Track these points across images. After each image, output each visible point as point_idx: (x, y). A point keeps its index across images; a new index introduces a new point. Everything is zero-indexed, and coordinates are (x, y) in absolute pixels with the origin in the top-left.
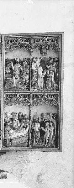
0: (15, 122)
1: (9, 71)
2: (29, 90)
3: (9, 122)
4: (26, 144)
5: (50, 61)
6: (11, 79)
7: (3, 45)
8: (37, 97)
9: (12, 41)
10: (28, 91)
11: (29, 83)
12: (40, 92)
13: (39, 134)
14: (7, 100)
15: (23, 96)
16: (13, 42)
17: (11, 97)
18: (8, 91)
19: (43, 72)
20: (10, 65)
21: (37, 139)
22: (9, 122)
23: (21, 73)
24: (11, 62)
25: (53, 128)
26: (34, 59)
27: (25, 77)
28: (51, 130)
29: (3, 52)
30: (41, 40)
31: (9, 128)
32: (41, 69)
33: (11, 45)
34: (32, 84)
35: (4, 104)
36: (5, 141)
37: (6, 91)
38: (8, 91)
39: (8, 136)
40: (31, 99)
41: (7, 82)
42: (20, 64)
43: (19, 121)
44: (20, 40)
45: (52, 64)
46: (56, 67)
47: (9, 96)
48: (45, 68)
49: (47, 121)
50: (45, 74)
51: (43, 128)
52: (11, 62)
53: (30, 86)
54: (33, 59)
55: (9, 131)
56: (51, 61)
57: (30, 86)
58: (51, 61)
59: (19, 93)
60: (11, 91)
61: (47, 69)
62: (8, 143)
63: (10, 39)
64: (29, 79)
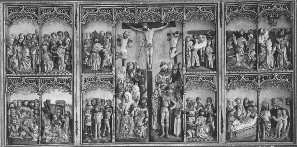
0: (239, 110)
1: (231, 47)
2: (256, 69)
3: (232, 110)
4: (254, 138)
5: (281, 33)
6: (234, 57)
7: (223, 14)
8: (266, 78)
9: (234, 8)
10: (255, 72)
11: (256, 61)
12: (269, 71)
13: (270, 125)
14: (230, 83)
15: (249, 77)
16: (236, 10)
17: (234, 80)
18: (231, 72)
19: (273, 47)
20: (233, 39)
21: (268, 131)
22: (232, 110)
23: (246, 50)
24: (233, 35)
25: (287, 117)
26: (262, 31)
27: (251, 54)
28: (284, 119)
29: (223, 23)
30: (270, 6)
31: (232, 118)
32: (270, 44)
33: (233, 14)
34: (259, 62)
35: (226, 88)
36: (228, 135)
37: (228, 72)
38: (231, 72)
39: (232, 127)
40: (259, 81)
41: (229, 60)
42: (244, 37)
43: (244, 109)
44: (244, 7)
45: (284, 36)
46: (288, 40)
47: (232, 77)
48: (275, 42)
49: (279, 109)
50: (275, 49)
51: (274, 117)
52: (233, 35)
53: (258, 65)
54: (260, 30)
55: (232, 122)
56: (282, 33)
57: (258, 65)
58: (282, 33)
59: (244, 74)
60: (234, 72)
61: (278, 43)
62: (231, 137)
63: (232, 6)
64: (256, 56)
